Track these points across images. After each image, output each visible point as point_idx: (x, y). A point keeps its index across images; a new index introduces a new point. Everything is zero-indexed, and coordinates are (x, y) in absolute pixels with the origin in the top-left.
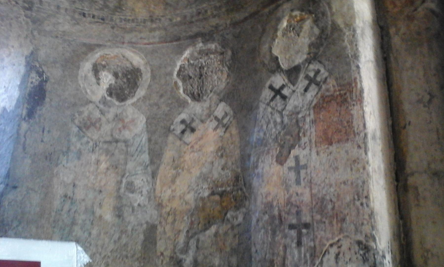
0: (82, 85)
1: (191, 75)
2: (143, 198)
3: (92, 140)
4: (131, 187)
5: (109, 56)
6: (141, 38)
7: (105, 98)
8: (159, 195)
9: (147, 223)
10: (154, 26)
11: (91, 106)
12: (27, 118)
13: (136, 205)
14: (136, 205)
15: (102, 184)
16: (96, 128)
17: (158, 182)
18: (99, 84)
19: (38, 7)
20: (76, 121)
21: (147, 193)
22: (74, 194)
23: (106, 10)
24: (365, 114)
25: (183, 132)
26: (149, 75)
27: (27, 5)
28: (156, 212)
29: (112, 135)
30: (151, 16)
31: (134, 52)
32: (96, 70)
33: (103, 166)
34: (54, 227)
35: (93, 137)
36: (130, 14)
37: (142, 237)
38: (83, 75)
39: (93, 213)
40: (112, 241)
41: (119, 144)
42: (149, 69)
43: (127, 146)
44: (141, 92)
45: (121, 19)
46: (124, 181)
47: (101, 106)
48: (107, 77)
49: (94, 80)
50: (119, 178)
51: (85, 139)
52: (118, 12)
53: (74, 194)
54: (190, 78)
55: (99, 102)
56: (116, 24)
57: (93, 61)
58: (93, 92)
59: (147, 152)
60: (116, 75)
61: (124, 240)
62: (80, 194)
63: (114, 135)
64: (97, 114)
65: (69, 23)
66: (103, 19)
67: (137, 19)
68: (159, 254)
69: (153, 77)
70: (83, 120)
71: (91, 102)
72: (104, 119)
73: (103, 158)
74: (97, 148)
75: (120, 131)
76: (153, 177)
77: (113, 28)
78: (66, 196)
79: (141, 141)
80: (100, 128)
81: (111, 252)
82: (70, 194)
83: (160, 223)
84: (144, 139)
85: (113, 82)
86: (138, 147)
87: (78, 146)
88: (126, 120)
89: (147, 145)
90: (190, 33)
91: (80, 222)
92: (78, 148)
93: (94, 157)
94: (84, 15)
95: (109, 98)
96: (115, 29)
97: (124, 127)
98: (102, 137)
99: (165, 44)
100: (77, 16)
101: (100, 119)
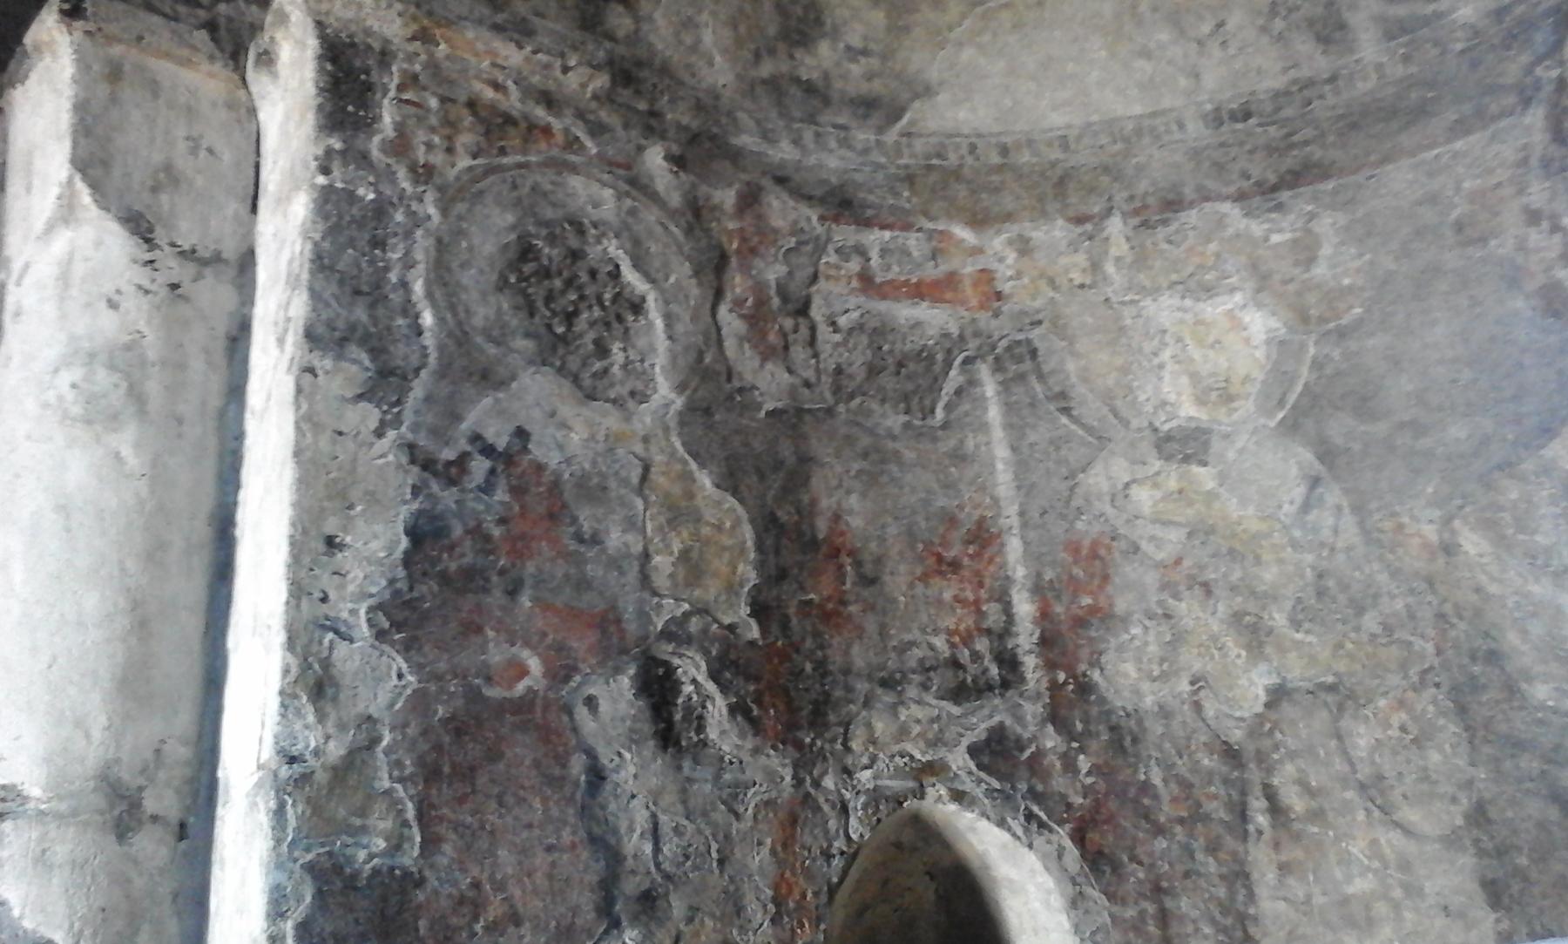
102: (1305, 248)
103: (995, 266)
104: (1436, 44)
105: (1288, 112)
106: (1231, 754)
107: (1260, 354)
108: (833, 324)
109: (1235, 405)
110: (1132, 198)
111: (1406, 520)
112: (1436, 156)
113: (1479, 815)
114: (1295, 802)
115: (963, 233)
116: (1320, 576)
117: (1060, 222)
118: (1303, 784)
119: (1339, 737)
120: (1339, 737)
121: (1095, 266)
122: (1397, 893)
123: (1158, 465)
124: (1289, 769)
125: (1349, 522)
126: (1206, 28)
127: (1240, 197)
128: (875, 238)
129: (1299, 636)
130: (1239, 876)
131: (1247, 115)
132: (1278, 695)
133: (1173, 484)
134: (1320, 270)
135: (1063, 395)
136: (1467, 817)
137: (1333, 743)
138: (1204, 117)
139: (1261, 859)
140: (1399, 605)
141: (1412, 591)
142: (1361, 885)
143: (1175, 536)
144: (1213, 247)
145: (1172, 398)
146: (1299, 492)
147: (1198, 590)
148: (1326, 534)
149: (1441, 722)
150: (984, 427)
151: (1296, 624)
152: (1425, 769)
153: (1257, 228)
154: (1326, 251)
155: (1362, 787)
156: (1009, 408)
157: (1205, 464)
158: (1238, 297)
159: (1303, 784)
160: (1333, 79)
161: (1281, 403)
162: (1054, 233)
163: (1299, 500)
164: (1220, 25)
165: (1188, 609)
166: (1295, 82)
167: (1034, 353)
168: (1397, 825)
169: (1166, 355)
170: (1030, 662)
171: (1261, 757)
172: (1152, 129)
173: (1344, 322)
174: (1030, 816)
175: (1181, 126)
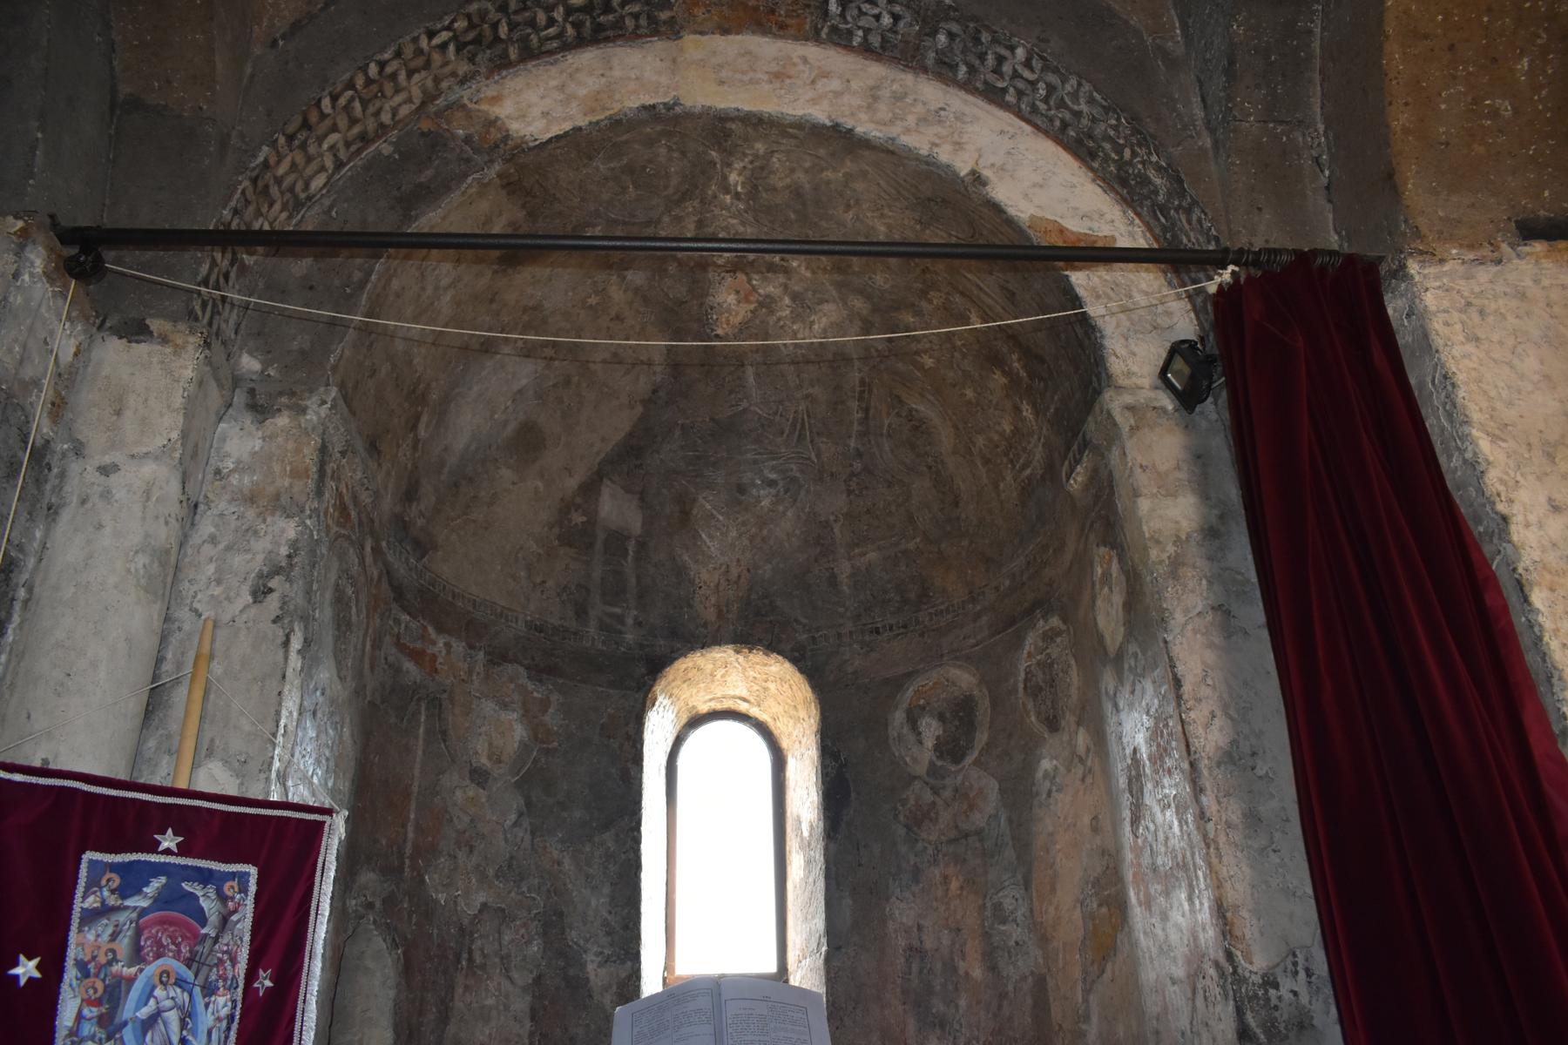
0: (897, 754)
1: (1041, 684)
2: (1019, 929)
4: (1000, 915)
5: (927, 687)
6: (964, 638)
7: (934, 765)
8: (1039, 920)
9: (1032, 973)
11: (917, 785)
12: (832, 834)
13: (1012, 943)
15: (959, 917)
16: (931, 820)
18: (921, 742)
19: (812, 650)
20: (901, 818)
22: (921, 942)
23: (906, 608)
24: (1186, 727)
26: (987, 702)
27: (797, 654)
29: (957, 827)
30: (970, 593)
31: (960, 667)
32: (912, 721)
34: (904, 1004)
35: (931, 838)
36: (940, 600)
37: (1029, 1001)
38: (896, 735)
39: (955, 969)
40: (990, 1016)
41: (970, 840)
43: (981, 840)
44: (982, 737)
45: (930, 614)
46: (989, 905)
47: (932, 781)
48: (930, 725)
49: (911, 738)
50: (980, 902)
51: (920, 845)
52: (925, 604)
53: (921, 942)
54: (1041, 689)
55: (928, 774)
56: (925, 627)
57: (905, 705)
58: (915, 760)
59: (1010, 843)
60: (941, 717)
62: (929, 944)
63: (960, 824)
64: (928, 796)
65: (859, 654)
66: (905, 627)
67: (953, 606)
68: (1057, 1028)
70: (911, 812)
71: (915, 778)
72: (939, 802)
73: (951, 870)
74: (940, 856)
75: (967, 816)
76: (1026, 889)
77: (922, 635)
78: (911, 949)
79: (999, 825)
80: (937, 819)
81: (992, 1034)
82: (916, 943)
84: (1002, 820)
86: (997, 838)
87: (913, 859)
89: (1008, 832)
90: (1026, 605)
92: (912, 863)
93: (936, 873)
94: (878, 632)
95: (939, 763)
96: (926, 636)
97: (971, 807)
98: (944, 834)
99: (998, 637)
100: (867, 638)
101: (934, 803)
102: (545, 704)
103: (437, 654)
104: (616, 643)
105: (556, 638)
106: (462, 930)
107: (516, 745)
108: (386, 659)
109: (501, 765)
110: (489, 646)
111: (548, 845)
112: (602, 692)
113: (538, 980)
114: (478, 959)
115: (430, 629)
116: (512, 858)
117: (464, 644)
118: (482, 950)
119: (499, 933)
120: (499, 933)
121: (470, 672)
122: (501, 1008)
123: (468, 782)
124: (479, 943)
125: (528, 837)
126: (538, 580)
127: (527, 668)
128: (405, 617)
129: (496, 883)
130: (451, 988)
131: (540, 632)
132: (484, 905)
133: (471, 794)
134: (547, 718)
135: (444, 733)
136: (534, 980)
137: (497, 935)
138: (526, 622)
139: (460, 979)
140: (536, 881)
141: (542, 877)
142: (490, 1001)
143: (466, 819)
144: (512, 686)
145: (480, 752)
146: (513, 817)
147: (467, 848)
148: (518, 840)
149: (536, 937)
150: (417, 738)
151: (497, 877)
152: (525, 956)
153: (530, 686)
154: (551, 710)
155: (502, 958)
156: (427, 732)
157: (484, 789)
158: (515, 715)
159: (482, 950)
160: (575, 634)
161: (519, 771)
162: (459, 647)
163: (513, 820)
164: (544, 582)
165: (461, 856)
166: (562, 626)
167: (441, 705)
168: (510, 978)
169: (483, 729)
170: (407, 862)
171: (472, 934)
172: (507, 616)
173: (550, 746)
174: (394, 940)
175: (517, 621)
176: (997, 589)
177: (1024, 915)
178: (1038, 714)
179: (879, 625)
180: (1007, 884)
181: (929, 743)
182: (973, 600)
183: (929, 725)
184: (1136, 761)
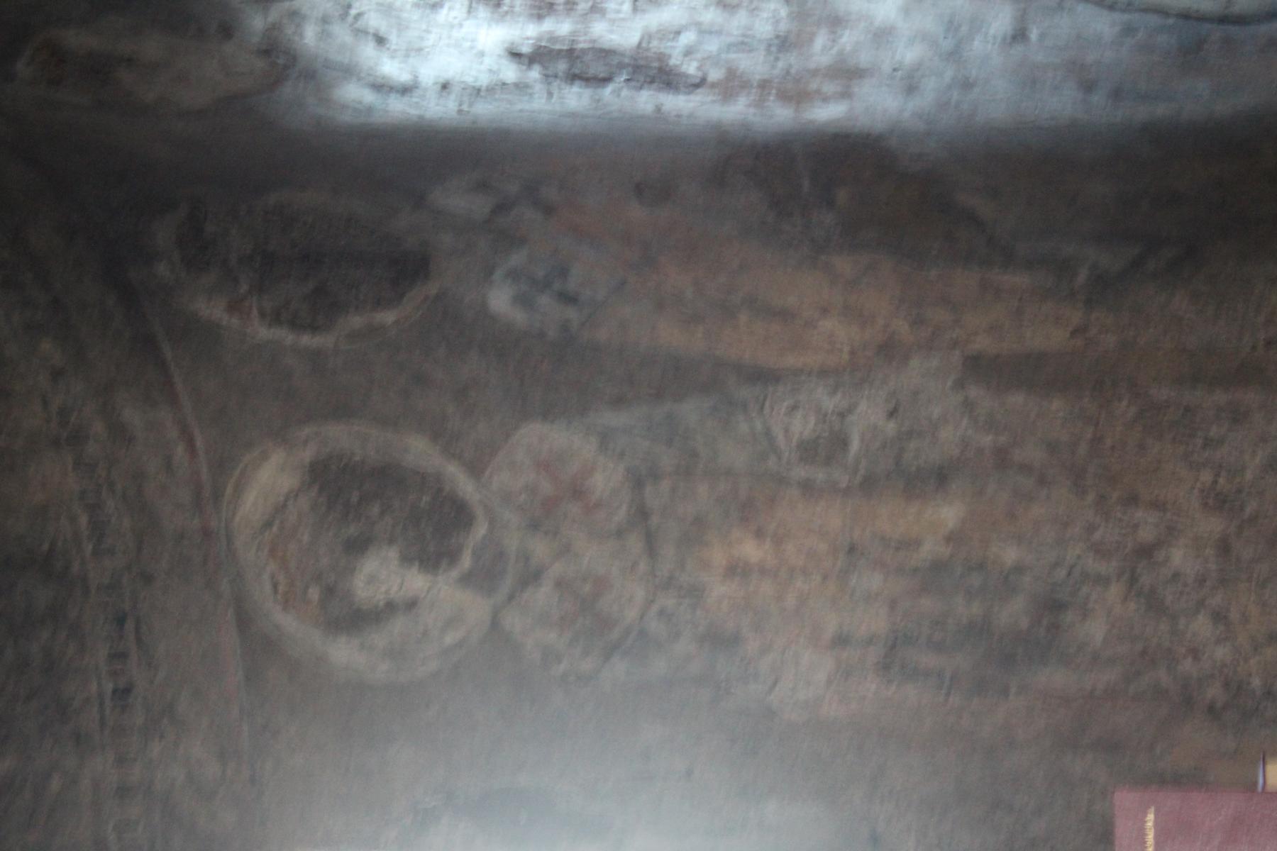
3: (649, 603)
5: (281, 578)
9: (960, 385)
10: (98, 427)
11: (514, 621)
13: (891, 427)
14: (891, 427)
17: (791, 361)
21: (839, 395)
25: (568, 299)
28: (915, 362)
29: (620, 534)
31: (239, 490)
33: (751, 550)
37: (1017, 399)
42: (307, 431)
43: (655, 475)
45: (96, 553)
46: (800, 472)
49: (398, 625)
51: (655, 626)
60: (358, 546)
61: (1032, 453)
64: (542, 595)
66: (121, 621)
69: (342, 411)
71: (495, 624)
73: (718, 556)
83: (955, 344)
85: (393, 553)
88: (547, 487)
91: (976, 609)
93: (719, 590)
95: (466, 561)
101: (560, 584)
176: (57, 375)
177: (834, 392)
178: (379, 304)
179: (109, 687)
180: (759, 426)
181: (416, 581)
182: (77, 438)
183: (372, 579)
184: (539, 56)
